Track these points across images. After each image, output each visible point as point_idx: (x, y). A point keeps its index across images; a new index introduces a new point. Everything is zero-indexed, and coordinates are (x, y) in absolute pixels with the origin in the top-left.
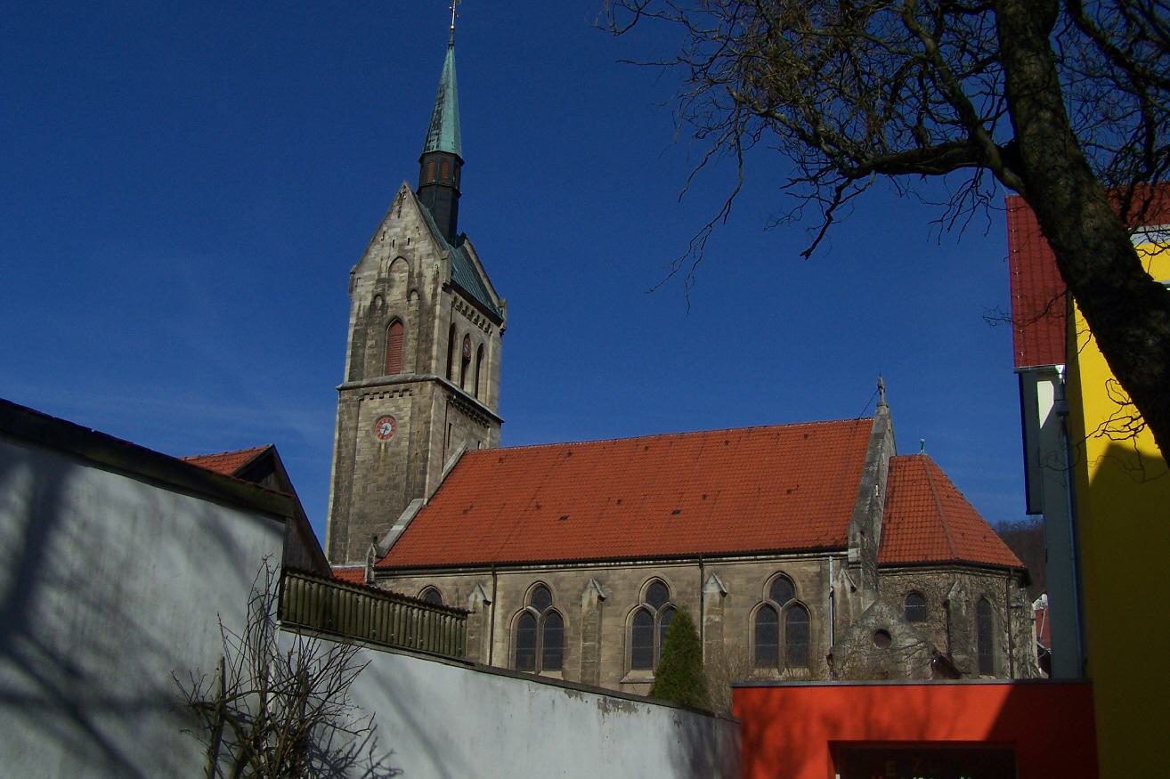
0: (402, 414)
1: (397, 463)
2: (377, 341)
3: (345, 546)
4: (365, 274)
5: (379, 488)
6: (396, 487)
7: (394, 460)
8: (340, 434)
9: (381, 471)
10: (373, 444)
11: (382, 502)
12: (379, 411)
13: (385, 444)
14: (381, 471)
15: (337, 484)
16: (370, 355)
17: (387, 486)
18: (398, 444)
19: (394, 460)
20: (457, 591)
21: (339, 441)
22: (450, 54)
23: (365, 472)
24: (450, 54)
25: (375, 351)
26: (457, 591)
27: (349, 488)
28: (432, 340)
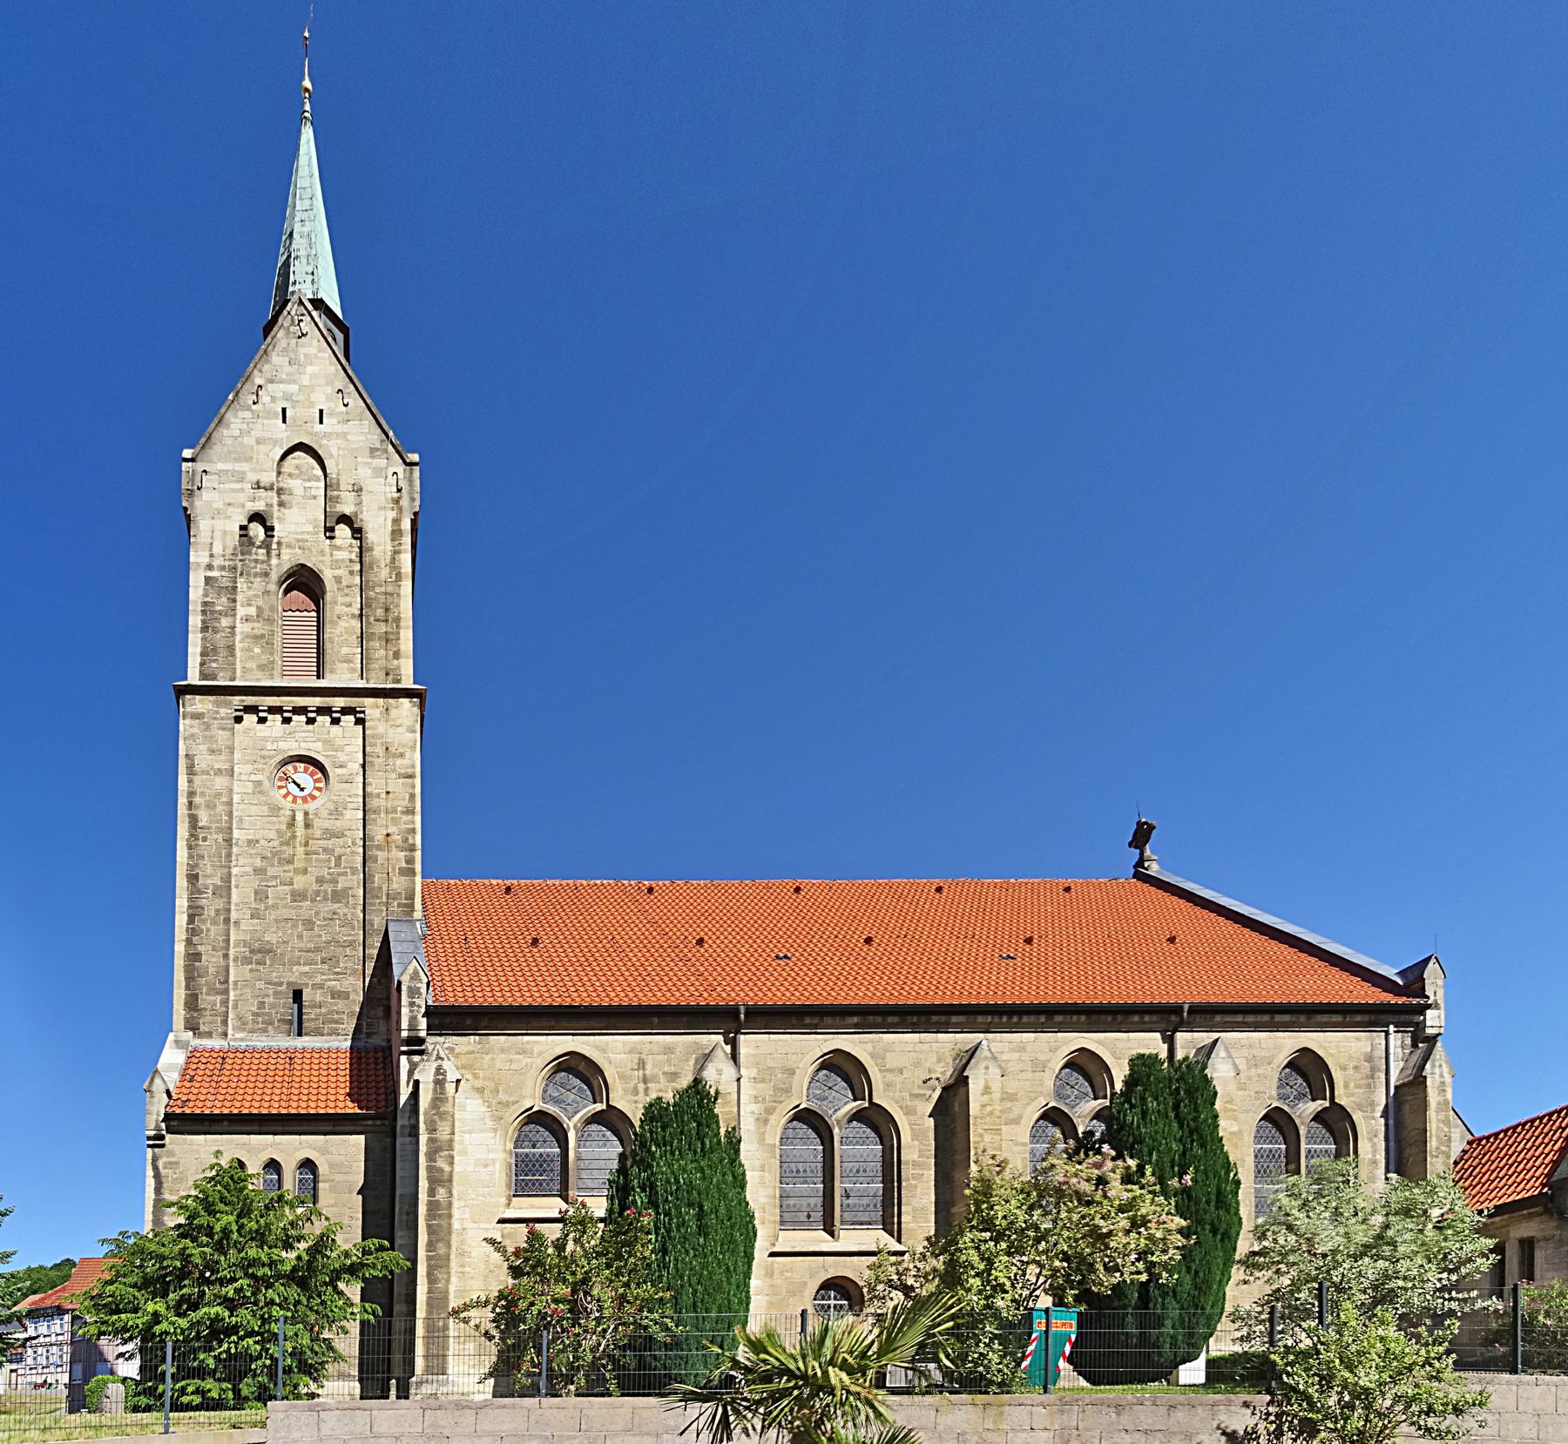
0: (342, 757)
1: (338, 851)
2: (258, 608)
3: (225, 1002)
4: (220, 466)
5: (298, 896)
6: (337, 896)
7: (330, 844)
8: (190, 781)
9: (298, 864)
10: (275, 810)
11: (309, 924)
12: (282, 745)
13: (306, 814)
14: (298, 864)
15: (193, 878)
16: (247, 636)
17: (317, 893)
18: (337, 812)
19: (330, 844)
20: (642, 1064)
21: (191, 794)
22: (307, 134)
23: (258, 862)
24: (307, 134)
25: (259, 628)
26: (642, 1064)
27: (224, 890)
28: (398, 620)
